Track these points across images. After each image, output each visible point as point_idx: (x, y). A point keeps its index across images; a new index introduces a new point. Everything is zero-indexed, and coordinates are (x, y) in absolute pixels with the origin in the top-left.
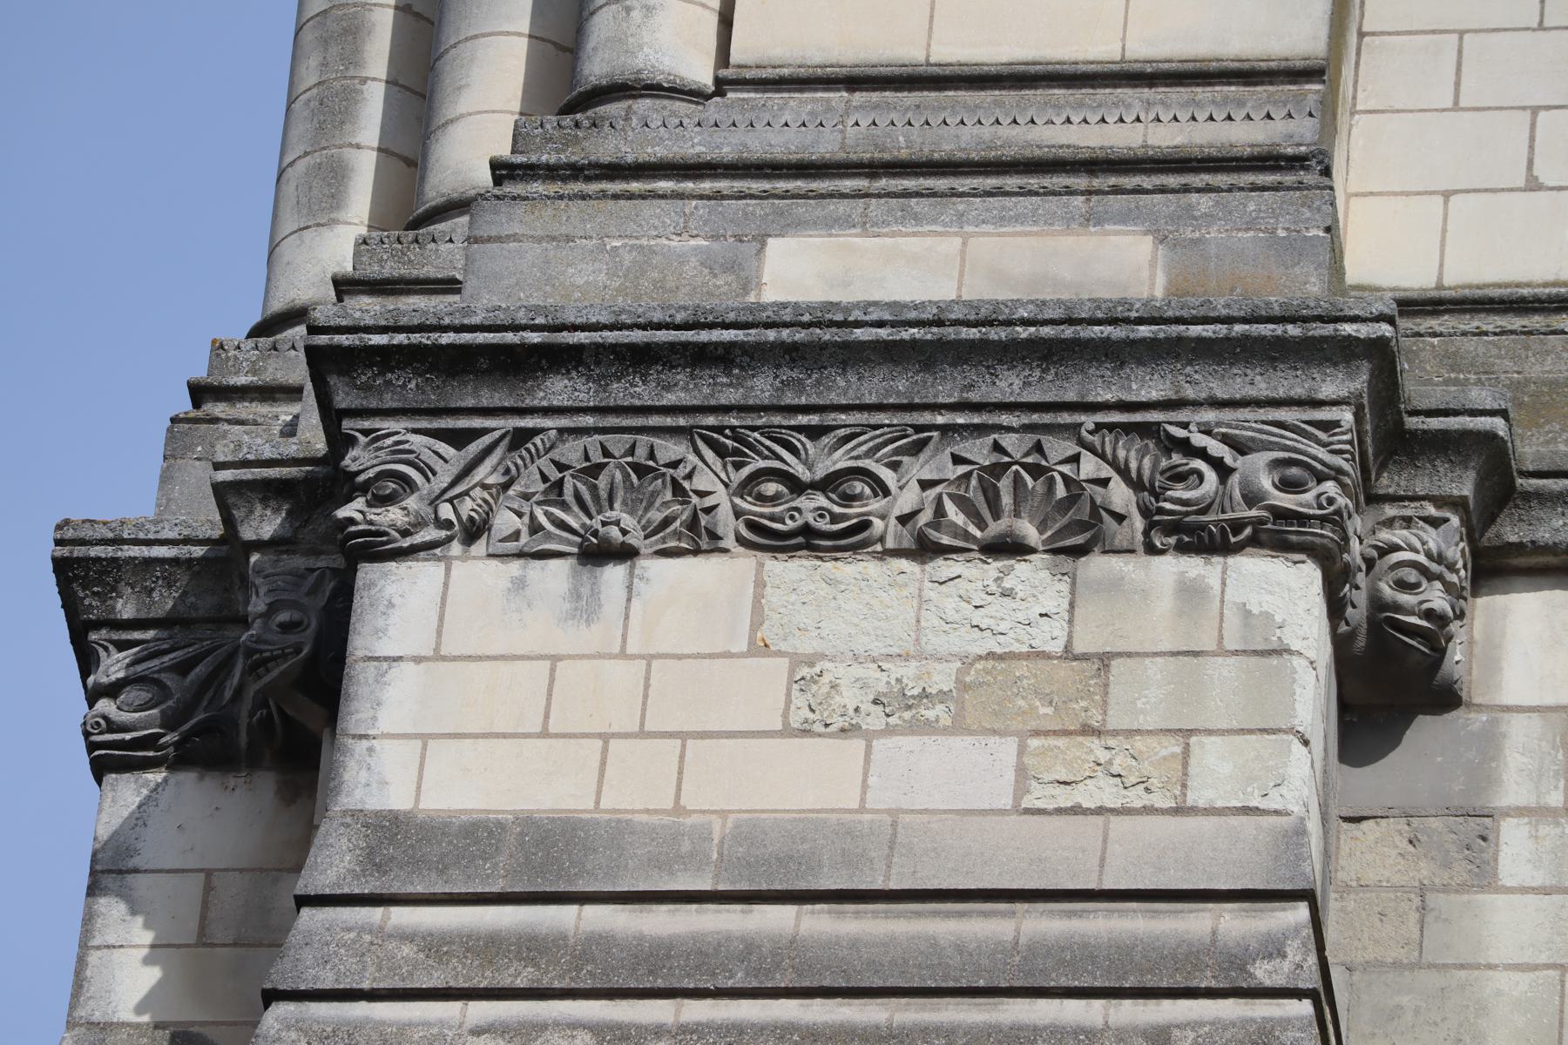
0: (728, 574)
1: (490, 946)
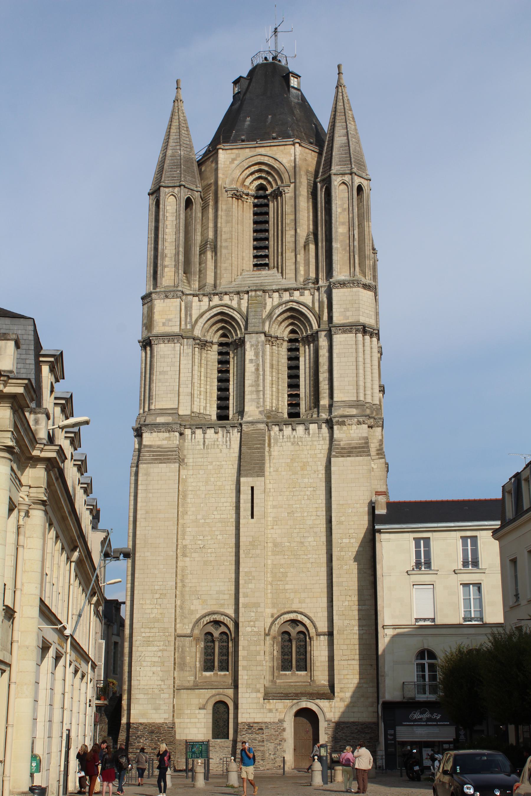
0: (156, 433)
1: (148, 451)
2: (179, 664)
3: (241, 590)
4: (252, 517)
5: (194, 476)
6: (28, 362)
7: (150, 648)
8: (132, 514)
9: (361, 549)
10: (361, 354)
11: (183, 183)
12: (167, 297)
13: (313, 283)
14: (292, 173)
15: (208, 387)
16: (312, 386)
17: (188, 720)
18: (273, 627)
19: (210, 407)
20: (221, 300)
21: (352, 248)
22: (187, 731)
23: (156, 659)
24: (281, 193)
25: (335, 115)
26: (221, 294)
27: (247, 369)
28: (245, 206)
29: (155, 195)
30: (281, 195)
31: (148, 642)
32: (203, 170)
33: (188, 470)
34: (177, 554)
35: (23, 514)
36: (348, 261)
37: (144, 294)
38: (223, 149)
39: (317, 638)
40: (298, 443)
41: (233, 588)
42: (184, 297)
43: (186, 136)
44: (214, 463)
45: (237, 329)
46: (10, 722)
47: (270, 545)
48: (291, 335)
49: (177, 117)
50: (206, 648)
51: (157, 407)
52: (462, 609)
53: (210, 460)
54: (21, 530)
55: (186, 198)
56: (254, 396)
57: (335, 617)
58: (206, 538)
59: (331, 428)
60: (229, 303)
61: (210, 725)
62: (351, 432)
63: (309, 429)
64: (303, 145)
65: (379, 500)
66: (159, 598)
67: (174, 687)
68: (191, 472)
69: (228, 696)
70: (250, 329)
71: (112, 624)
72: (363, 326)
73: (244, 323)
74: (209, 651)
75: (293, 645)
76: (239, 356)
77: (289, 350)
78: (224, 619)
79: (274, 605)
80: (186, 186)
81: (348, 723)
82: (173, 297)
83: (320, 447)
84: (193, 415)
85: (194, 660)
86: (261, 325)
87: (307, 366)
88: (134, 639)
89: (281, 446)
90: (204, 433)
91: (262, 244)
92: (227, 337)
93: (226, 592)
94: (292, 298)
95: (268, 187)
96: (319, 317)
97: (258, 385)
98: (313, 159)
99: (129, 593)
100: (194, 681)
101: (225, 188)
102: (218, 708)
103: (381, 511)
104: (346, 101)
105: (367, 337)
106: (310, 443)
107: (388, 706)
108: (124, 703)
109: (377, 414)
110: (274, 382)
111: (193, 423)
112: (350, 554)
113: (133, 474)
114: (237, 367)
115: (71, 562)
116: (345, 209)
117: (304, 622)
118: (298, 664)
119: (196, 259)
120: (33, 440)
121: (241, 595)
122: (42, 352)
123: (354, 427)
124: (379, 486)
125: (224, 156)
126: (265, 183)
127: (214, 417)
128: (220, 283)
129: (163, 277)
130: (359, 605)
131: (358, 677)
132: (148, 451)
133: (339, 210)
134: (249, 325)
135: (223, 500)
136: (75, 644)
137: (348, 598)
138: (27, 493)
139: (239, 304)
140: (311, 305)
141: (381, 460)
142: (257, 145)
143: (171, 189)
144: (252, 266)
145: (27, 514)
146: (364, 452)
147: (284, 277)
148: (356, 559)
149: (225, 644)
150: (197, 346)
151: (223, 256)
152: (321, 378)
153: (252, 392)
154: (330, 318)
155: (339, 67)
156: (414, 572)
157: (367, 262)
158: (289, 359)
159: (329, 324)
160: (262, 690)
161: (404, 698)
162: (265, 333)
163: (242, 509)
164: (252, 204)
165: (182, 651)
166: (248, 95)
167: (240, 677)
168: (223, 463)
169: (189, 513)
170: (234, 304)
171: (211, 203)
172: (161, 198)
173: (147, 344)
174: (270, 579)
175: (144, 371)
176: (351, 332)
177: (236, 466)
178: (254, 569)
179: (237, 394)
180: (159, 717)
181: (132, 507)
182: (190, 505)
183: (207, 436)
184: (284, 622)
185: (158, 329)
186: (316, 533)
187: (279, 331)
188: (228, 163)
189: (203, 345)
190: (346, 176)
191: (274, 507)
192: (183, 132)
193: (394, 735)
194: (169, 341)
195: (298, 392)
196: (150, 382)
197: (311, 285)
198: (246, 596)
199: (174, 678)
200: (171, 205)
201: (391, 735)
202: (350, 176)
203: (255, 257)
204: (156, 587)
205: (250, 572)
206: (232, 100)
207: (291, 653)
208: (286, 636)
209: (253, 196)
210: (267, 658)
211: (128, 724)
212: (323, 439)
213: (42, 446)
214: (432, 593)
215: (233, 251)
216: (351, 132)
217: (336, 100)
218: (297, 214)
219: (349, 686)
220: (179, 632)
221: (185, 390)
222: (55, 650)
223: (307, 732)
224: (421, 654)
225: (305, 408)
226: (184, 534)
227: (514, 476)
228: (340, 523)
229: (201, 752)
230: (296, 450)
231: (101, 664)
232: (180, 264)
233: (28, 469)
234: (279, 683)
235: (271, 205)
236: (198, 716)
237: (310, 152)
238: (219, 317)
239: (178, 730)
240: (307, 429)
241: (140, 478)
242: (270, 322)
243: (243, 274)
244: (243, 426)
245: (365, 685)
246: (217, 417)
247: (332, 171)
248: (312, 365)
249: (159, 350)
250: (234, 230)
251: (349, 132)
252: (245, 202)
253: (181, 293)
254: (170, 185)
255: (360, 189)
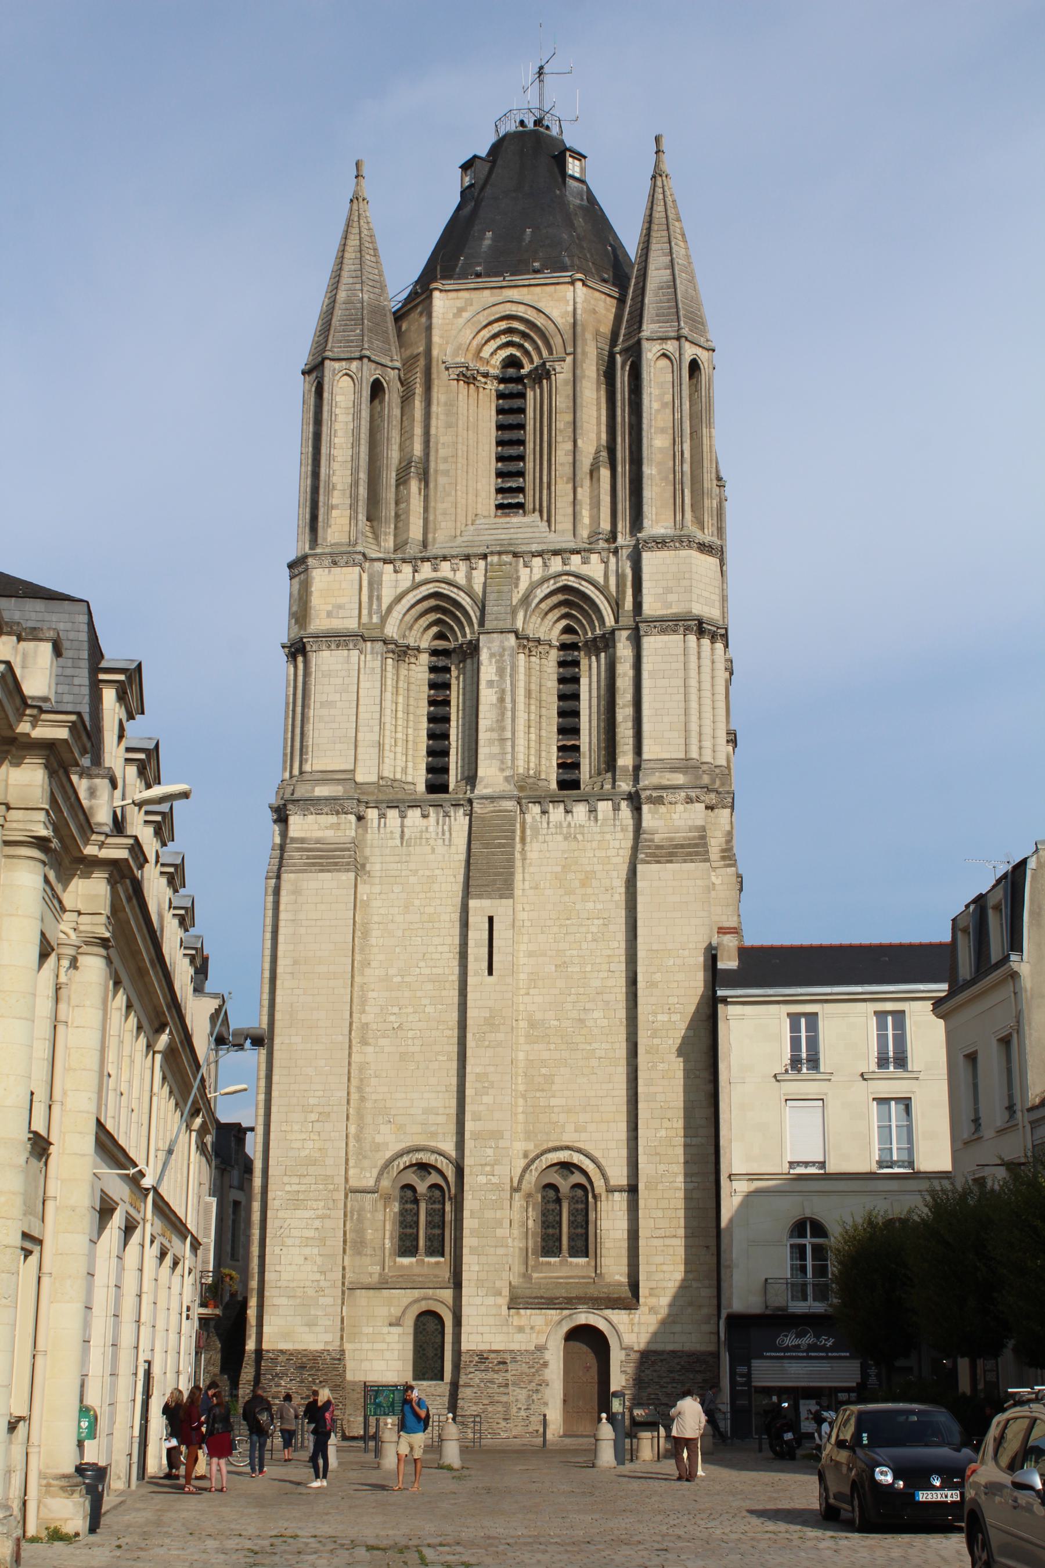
0: (314, 816)
2: (354, 1243)
3: (468, 1108)
4: (490, 972)
5: (383, 896)
6: (76, 681)
7: (299, 1213)
8: (267, 966)
9: (691, 1033)
10: (693, 673)
11: (367, 353)
12: (335, 563)
13: (607, 541)
14: (568, 336)
15: (410, 731)
16: (602, 731)
17: (368, 1346)
18: (527, 1176)
19: (415, 769)
20: (435, 570)
21: (678, 476)
22: (366, 1365)
23: (311, 1233)
24: (548, 372)
25: (649, 229)
26: (436, 558)
27: (482, 699)
28: (481, 395)
29: (314, 375)
30: (549, 378)
31: (296, 1202)
32: (404, 328)
33: (372, 884)
34: (350, 1041)
35: (65, 963)
36: (672, 501)
37: (292, 557)
38: (441, 291)
39: (607, 1197)
40: (575, 837)
41: (454, 1103)
42: (367, 564)
43: (373, 265)
44: (421, 872)
45: (465, 623)
46: (40, 1346)
47: (523, 1024)
48: (565, 637)
49: (356, 231)
50: (403, 1213)
51: (316, 768)
52: (876, 1146)
53: (412, 866)
54: (63, 992)
55: (371, 380)
56: (496, 749)
57: (641, 1159)
58: (404, 1011)
59: (637, 810)
60: (449, 575)
61: (410, 1355)
62: (675, 816)
63: (596, 811)
64: (589, 283)
65: (725, 942)
66: (318, 1121)
67: (343, 1284)
68: (377, 889)
69: (442, 1302)
70: (488, 625)
71: (229, 1168)
72: (698, 620)
73: (478, 614)
74: (409, 1218)
75: (564, 1211)
76: (468, 674)
77: (561, 664)
78: (436, 1160)
79: (528, 1136)
80: (373, 357)
81: (662, 1353)
82: (347, 564)
83: (617, 844)
84: (384, 784)
85: (381, 1232)
86: (509, 616)
87: (595, 693)
88: (271, 1195)
89: (545, 842)
90: (403, 817)
91: (512, 467)
92: (447, 639)
93: (441, 1111)
94: (567, 568)
95: (525, 361)
96: (617, 604)
97: (503, 729)
98: (607, 310)
99: (261, 1112)
100: (380, 1275)
101: (444, 362)
102: (424, 1325)
103: (728, 963)
104: (670, 203)
105: (706, 642)
106: (598, 837)
107: (738, 1323)
108: (252, 1313)
109: (723, 784)
110: (533, 724)
111: (381, 797)
112: (671, 1042)
113: (270, 891)
114: (464, 695)
115: (154, 1053)
116: (667, 403)
117: (584, 1167)
118: (573, 1244)
119: (389, 494)
120: (86, 826)
121: (468, 1116)
122: (104, 664)
123: (680, 807)
124: (724, 918)
125: (442, 303)
126: (518, 354)
127: (421, 787)
128: (434, 539)
129: (329, 526)
130: (685, 1136)
131: (682, 1268)
132: (299, 850)
133: (656, 406)
134: (488, 617)
135: (436, 941)
136: (161, 1203)
137: (666, 1124)
138: (74, 925)
139: (469, 578)
140: (601, 580)
141: (728, 869)
142: (504, 284)
143: (344, 363)
144: (493, 508)
145: (74, 964)
146: (697, 854)
147: (553, 529)
148: (681, 1052)
149: (437, 1206)
150: (391, 655)
151: (440, 488)
152: (619, 718)
153: (491, 742)
154: (638, 605)
155: (658, 139)
156: (787, 1077)
157: (707, 502)
158: (561, 680)
159: (634, 616)
160: (506, 1292)
161: (767, 1307)
162: (516, 633)
163: (471, 958)
164: (494, 393)
165: (358, 1219)
166: (488, 190)
167: (464, 1267)
168: (437, 872)
169: (374, 964)
170: (460, 578)
171: (419, 390)
172: (326, 380)
173: (297, 650)
174: (521, 1088)
175: (291, 700)
176: (675, 632)
177: (461, 878)
178: (492, 1069)
179: (463, 746)
180: (314, 1339)
181: (268, 952)
182: (375, 950)
183: (408, 822)
184: (547, 1167)
185: (319, 623)
186: (607, 1003)
187: (543, 629)
188: (451, 316)
189: (402, 653)
190: (669, 342)
191: (531, 954)
192: (368, 257)
193: (748, 1375)
194: (338, 646)
195: (577, 743)
196: (302, 721)
197: (602, 544)
198: (477, 1118)
199: (344, 1268)
200: (344, 393)
201: (742, 1376)
202: (676, 343)
203: (500, 491)
204: (312, 1101)
205: (486, 1074)
206: (459, 199)
207: (560, 1223)
208: (551, 1193)
209: (496, 378)
210: (516, 1232)
211: (259, 1352)
212: (622, 830)
213: (102, 838)
214: (821, 1114)
215: (459, 479)
216: (679, 261)
217: (652, 202)
218: (577, 413)
219: (665, 1284)
220: (353, 1183)
221: (368, 737)
222: (124, 1214)
223: (588, 1369)
224: (799, 1228)
225: (590, 771)
226: (364, 1002)
227: (974, 901)
228: (653, 985)
229: (392, 1404)
230: (573, 850)
231: (209, 1241)
232: (360, 503)
233: (75, 880)
234: (537, 1278)
235: (530, 394)
236: (388, 1339)
237: (603, 296)
238: (432, 602)
239: (350, 1364)
240: (593, 811)
241: (284, 899)
242: (526, 612)
243: (477, 522)
244: (475, 805)
245: (695, 1284)
246: (427, 787)
247: (643, 334)
248: (602, 692)
249: (319, 662)
250: (460, 440)
251: (676, 261)
252: (481, 390)
253: (361, 557)
254: (342, 356)
255: (694, 366)
